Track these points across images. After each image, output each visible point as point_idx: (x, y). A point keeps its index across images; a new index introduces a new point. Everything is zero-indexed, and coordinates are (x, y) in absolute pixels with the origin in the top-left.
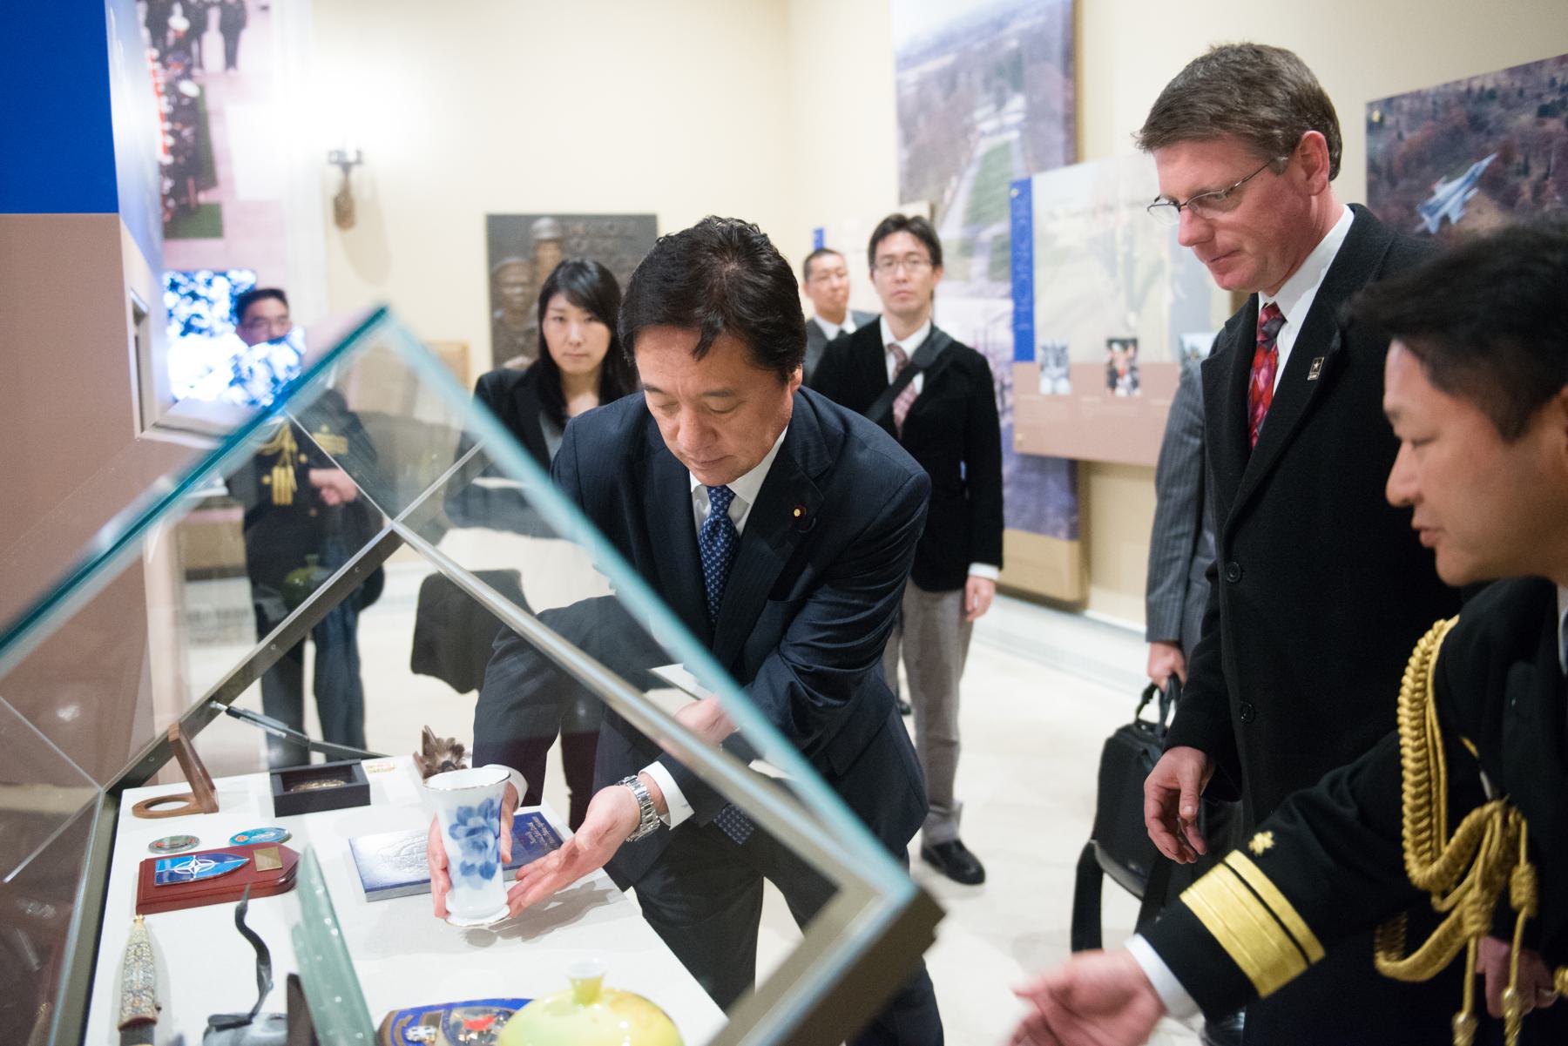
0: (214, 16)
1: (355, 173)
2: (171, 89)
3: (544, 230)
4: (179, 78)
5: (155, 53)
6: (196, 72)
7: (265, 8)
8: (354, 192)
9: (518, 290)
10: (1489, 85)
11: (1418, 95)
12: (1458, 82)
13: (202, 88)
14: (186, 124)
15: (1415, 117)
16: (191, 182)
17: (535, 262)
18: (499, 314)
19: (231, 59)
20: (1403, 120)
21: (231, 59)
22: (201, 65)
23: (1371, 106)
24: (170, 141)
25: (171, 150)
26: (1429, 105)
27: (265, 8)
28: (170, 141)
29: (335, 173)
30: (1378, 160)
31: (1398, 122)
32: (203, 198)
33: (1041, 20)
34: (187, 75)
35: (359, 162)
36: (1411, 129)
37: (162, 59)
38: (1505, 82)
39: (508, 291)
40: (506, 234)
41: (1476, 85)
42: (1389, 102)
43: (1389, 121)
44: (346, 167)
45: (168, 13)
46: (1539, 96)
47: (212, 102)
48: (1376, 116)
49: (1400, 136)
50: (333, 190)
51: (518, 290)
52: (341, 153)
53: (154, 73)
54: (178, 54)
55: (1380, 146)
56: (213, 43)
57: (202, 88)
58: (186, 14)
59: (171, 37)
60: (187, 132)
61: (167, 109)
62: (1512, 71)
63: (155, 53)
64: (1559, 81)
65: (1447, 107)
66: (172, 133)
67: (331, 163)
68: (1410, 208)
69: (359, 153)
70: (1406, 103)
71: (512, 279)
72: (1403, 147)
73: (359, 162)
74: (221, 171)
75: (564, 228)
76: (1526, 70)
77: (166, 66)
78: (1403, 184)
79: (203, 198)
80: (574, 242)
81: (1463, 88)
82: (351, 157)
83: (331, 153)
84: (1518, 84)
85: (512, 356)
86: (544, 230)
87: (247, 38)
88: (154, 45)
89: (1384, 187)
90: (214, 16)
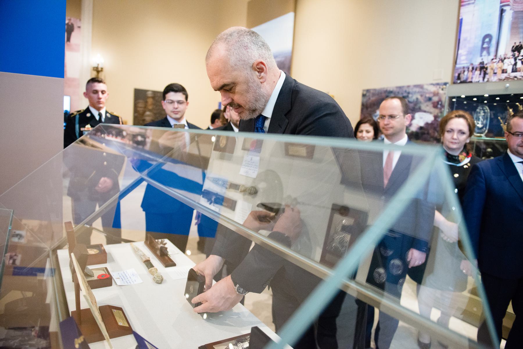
3: (149, 94)
7: (79, 27)
9: (141, 109)
10: (391, 90)
11: (375, 90)
12: (384, 88)
15: (374, 95)
17: (146, 102)
18: (136, 114)
20: (371, 95)
23: (364, 90)
26: (377, 92)
27: (79, 27)
30: (365, 104)
31: (369, 96)
33: (283, 59)
35: (102, 70)
36: (372, 97)
38: (395, 89)
39: (139, 109)
40: (140, 95)
41: (388, 89)
42: (368, 91)
43: (368, 94)
46: (402, 94)
48: (365, 93)
49: (369, 99)
51: (141, 109)
52: (97, 68)
55: (365, 100)
62: (397, 87)
64: (408, 90)
65: (381, 93)
67: (94, 70)
68: (371, 115)
69: (102, 68)
70: (372, 91)
72: (370, 101)
76: (400, 88)
78: (369, 109)
80: (157, 98)
81: (385, 89)
82: (100, 69)
83: (94, 68)
84: (398, 90)
86: (149, 94)
87: (74, 35)
89: (365, 110)
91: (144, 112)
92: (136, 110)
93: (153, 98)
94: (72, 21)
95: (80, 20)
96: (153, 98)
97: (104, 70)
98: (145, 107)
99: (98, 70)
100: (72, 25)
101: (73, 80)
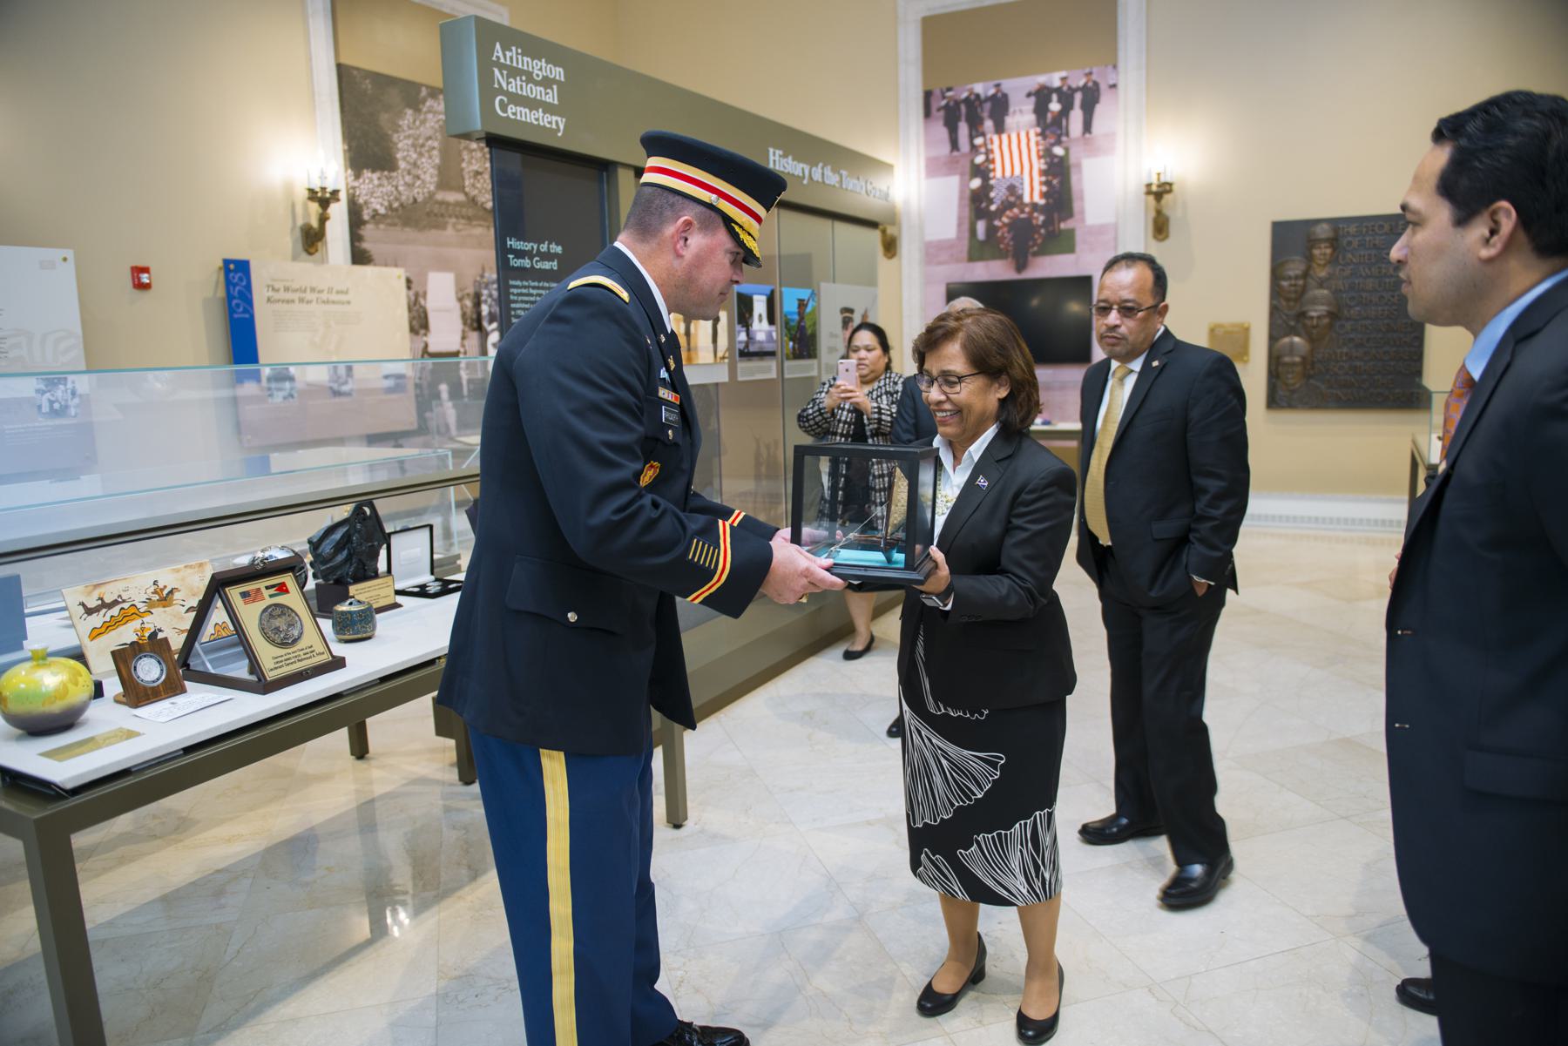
0: (1078, 97)
1: (1167, 197)
2: (1047, 154)
3: (1323, 231)
4: (1053, 145)
5: (1039, 130)
6: (1064, 139)
7: (1114, 86)
8: (1166, 211)
13: (1067, 150)
14: (1055, 176)
16: (1056, 216)
17: (1310, 258)
19: (1087, 127)
21: (1087, 127)
22: (1067, 134)
24: (1044, 189)
25: (1043, 195)
27: (1114, 86)
28: (1044, 189)
29: (1151, 198)
32: (1063, 226)
34: (1058, 142)
37: (1043, 135)
39: (1285, 284)
44: (1159, 196)
45: (1050, 101)
47: (1072, 160)
50: (1152, 214)
53: (1037, 144)
54: (1052, 127)
56: (1076, 116)
57: (1067, 150)
58: (1059, 101)
59: (1049, 116)
60: (1055, 182)
61: (1044, 167)
63: (1039, 130)
66: (1047, 183)
71: (1291, 273)
73: (1170, 191)
74: (1076, 206)
75: (1336, 230)
77: (1045, 138)
79: (1063, 226)
85: (1287, 335)
88: (1038, 124)
90: (1078, 97)
91: (1304, 289)
92: (1276, 291)
93: (1334, 242)
94: (1094, 77)
95: (1115, 67)
96: (1334, 242)
97: (1175, 187)
98: (1305, 275)
99: (1160, 192)
100: (1096, 84)
101: (1101, 230)
